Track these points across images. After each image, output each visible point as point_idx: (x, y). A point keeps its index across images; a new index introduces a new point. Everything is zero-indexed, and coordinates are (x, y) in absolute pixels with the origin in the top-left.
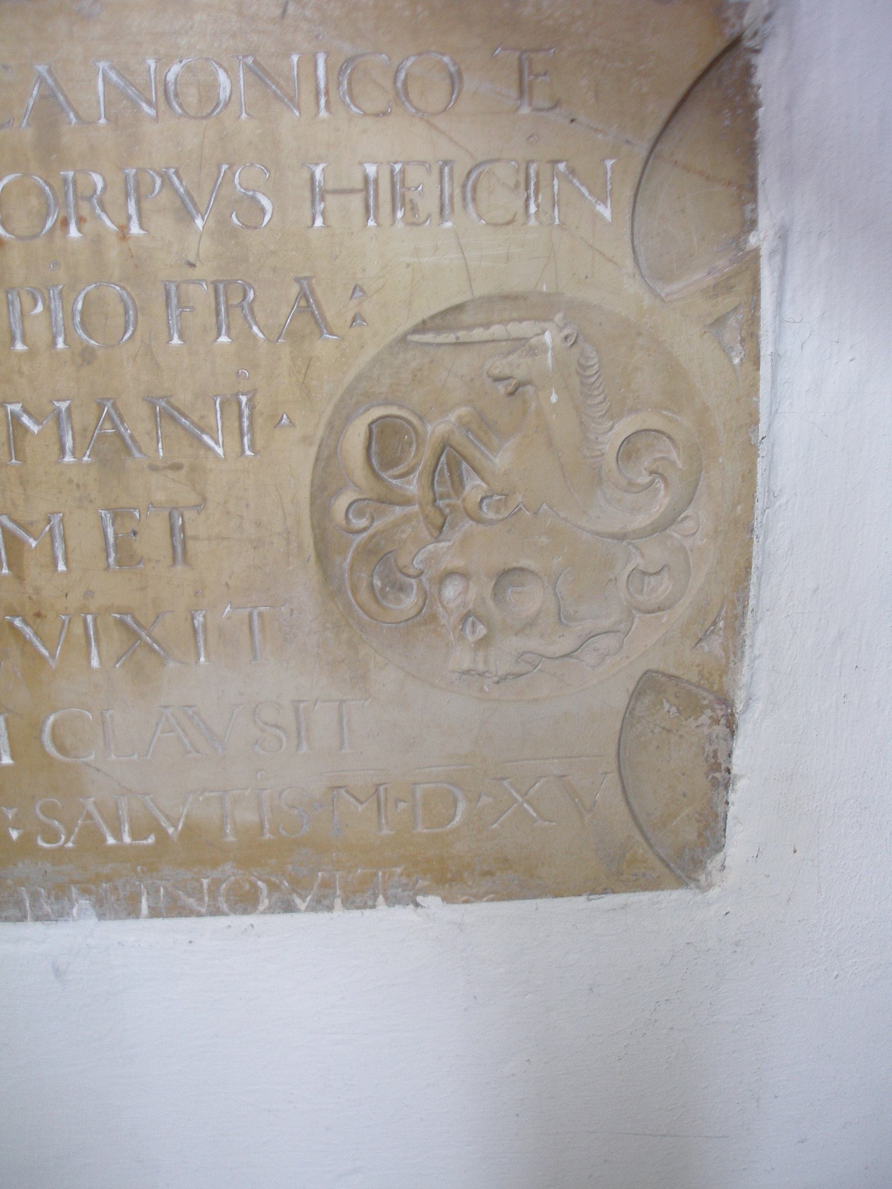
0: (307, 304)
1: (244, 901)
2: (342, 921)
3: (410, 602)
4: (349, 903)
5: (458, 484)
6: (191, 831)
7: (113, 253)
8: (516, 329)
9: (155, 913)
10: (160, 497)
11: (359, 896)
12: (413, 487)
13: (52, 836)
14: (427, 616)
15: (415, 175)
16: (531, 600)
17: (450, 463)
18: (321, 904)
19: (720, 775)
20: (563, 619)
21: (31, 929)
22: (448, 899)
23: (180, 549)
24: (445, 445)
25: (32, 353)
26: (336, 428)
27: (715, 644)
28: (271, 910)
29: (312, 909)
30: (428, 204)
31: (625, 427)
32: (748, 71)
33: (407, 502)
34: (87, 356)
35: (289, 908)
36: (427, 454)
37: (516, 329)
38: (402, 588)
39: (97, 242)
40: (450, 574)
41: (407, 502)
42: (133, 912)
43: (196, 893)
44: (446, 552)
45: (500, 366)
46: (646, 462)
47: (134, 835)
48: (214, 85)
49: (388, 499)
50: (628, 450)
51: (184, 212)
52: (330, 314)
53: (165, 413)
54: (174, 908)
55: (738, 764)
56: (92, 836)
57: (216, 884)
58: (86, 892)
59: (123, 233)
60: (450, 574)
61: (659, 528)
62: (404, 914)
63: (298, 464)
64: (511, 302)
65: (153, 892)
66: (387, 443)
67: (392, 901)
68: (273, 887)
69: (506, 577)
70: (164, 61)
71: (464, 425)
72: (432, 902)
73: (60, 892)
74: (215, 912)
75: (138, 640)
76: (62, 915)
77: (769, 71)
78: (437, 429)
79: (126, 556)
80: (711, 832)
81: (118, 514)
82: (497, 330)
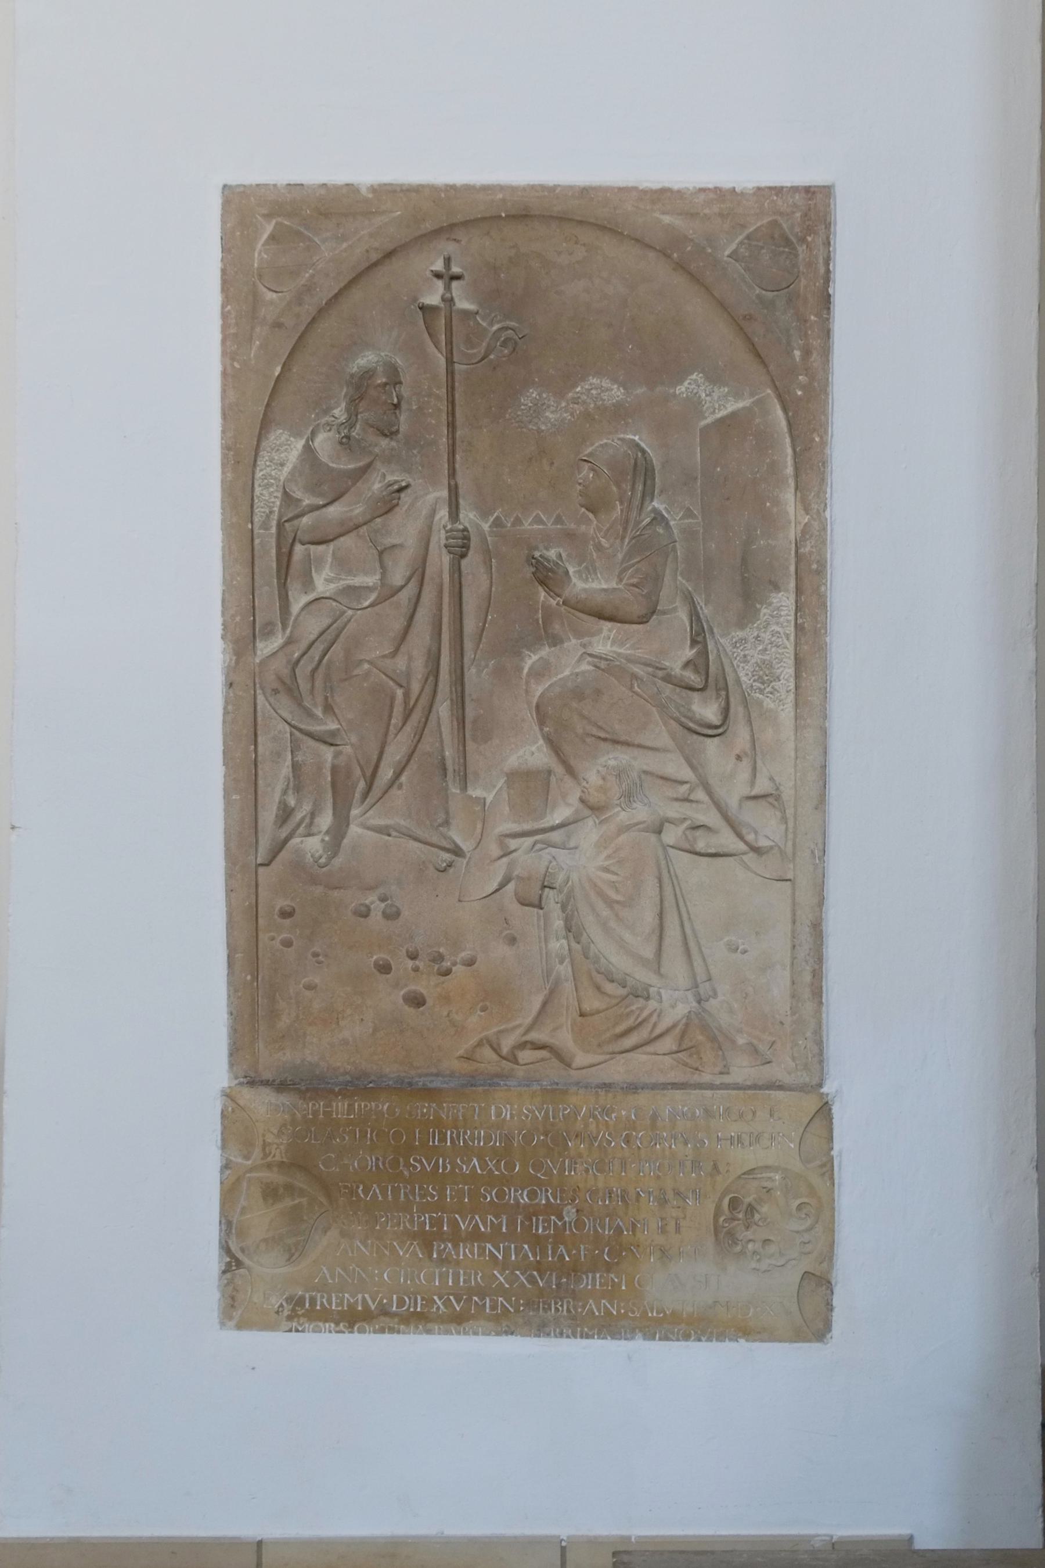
0: (715, 1167)
1: (687, 1337)
2: (715, 1345)
3: (739, 1248)
4: (717, 1340)
5: (753, 1216)
6: (673, 1313)
7: (667, 1153)
8: (768, 1175)
9: (660, 1339)
10: (674, 1215)
11: (721, 1337)
12: (741, 1216)
13: (633, 1312)
14: (742, 1253)
15: (744, 1136)
16: (772, 1249)
17: (751, 1209)
18: (709, 1340)
19: (830, 1308)
20: (781, 1255)
21: (623, 1342)
22: (747, 1341)
23: (678, 1229)
24: (750, 1205)
25: (644, 1176)
26: (721, 1199)
27: (825, 1265)
28: (694, 1340)
29: (707, 1341)
30: (747, 1143)
31: (798, 1202)
32: (830, 1109)
33: (739, 1220)
34: (658, 1177)
35: (700, 1340)
36: (745, 1207)
37: (768, 1175)
38: (737, 1244)
39: (663, 1150)
40: (750, 1240)
41: (739, 1220)
42: (654, 1339)
43: (673, 1333)
44: (749, 1234)
45: (765, 1184)
46: (805, 1211)
47: (658, 1313)
48: (695, 1113)
49: (734, 1219)
50: (799, 1208)
51: (686, 1144)
52: (721, 1169)
53: (678, 1193)
54: (666, 1338)
55: (835, 1303)
56: (645, 1312)
57: (679, 1330)
58: (641, 1331)
59: (670, 1147)
60: (750, 1240)
61: (809, 1229)
62: (733, 1345)
63: (711, 1207)
64: (767, 1168)
65: (660, 1332)
66: (734, 1203)
67: (730, 1340)
68: (696, 1333)
69: (766, 1242)
70: (683, 1106)
71: (755, 1200)
72: (742, 1341)
73: (633, 1331)
74: (678, 1340)
75: (664, 1254)
76: (632, 1338)
77: (835, 1110)
78: (748, 1200)
79: (663, 1230)
80: (828, 1326)
81: (662, 1219)
82: (764, 1175)
